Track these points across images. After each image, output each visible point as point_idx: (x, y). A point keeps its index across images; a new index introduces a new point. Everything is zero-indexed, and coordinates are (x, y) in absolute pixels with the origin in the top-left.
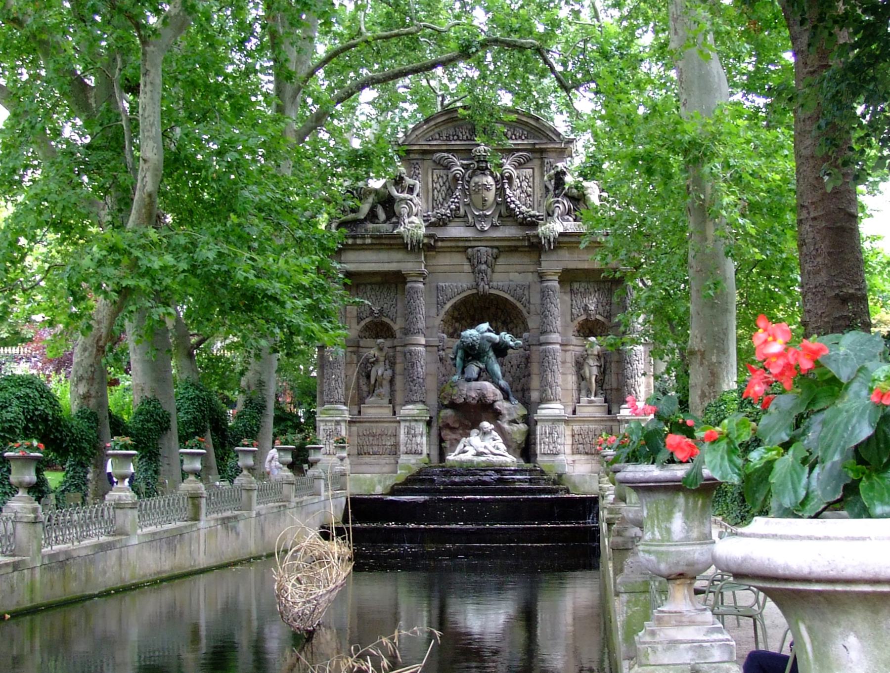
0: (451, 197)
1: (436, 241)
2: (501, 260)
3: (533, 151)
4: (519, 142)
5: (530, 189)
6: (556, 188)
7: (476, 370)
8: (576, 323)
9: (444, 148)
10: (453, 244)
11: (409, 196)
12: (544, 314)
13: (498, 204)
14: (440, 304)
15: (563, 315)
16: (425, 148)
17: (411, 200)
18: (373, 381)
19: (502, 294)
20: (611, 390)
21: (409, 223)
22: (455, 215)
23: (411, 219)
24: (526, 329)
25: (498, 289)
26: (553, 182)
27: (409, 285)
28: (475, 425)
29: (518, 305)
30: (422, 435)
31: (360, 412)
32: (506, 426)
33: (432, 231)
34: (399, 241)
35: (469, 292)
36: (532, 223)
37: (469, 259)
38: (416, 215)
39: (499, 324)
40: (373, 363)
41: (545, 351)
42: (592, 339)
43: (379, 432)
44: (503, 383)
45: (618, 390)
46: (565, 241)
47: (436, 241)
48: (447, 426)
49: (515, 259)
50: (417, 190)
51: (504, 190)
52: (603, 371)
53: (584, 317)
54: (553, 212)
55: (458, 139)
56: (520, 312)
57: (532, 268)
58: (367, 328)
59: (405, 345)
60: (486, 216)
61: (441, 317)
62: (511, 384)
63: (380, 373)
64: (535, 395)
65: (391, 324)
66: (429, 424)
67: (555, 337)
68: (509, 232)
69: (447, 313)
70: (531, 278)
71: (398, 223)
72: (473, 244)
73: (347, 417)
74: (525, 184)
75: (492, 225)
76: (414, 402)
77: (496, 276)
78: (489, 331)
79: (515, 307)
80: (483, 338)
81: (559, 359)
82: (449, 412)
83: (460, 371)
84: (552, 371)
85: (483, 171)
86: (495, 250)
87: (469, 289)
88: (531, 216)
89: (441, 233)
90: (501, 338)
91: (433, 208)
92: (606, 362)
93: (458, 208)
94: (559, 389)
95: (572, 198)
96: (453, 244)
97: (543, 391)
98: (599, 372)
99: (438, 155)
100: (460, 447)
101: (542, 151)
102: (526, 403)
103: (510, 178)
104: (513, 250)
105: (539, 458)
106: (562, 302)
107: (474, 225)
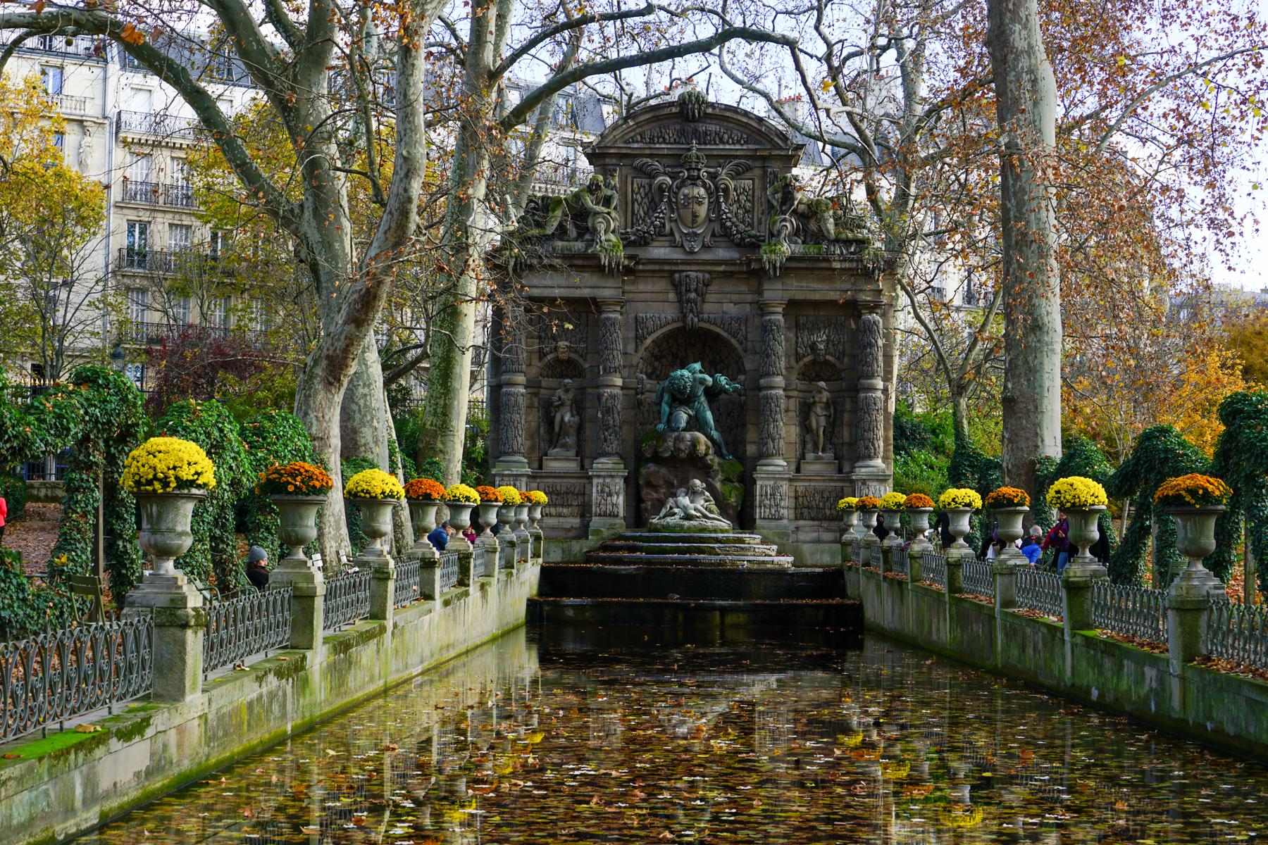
0: (655, 211)
1: (637, 263)
2: (712, 288)
3: (753, 157)
4: (738, 147)
5: (749, 204)
6: (783, 203)
7: (685, 416)
9: (647, 152)
10: (657, 267)
11: (606, 210)
12: (766, 353)
13: (711, 221)
14: (639, 339)
15: (787, 356)
16: (624, 151)
17: (609, 213)
18: (557, 429)
19: (712, 328)
20: (843, 444)
22: (660, 232)
24: (741, 370)
25: (709, 321)
26: (779, 196)
27: (604, 315)
28: (685, 483)
29: (733, 341)
30: (618, 495)
31: (540, 467)
32: (718, 485)
33: (631, 251)
34: (594, 262)
35: (675, 325)
36: (755, 246)
37: (676, 286)
38: (613, 232)
39: (706, 364)
40: (558, 406)
41: (767, 397)
42: (822, 384)
43: (564, 489)
44: (715, 434)
45: (852, 444)
46: (793, 267)
47: (637, 263)
48: (649, 484)
49: (729, 286)
50: (615, 203)
51: (719, 204)
52: (833, 424)
54: (779, 233)
55: (664, 142)
56: (735, 349)
57: (749, 298)
58: (550, 366)
59: (598, 387)
60: (695, 234)
61: (640, 355)
62: (722, 433)
63: (567, 418)
64: (751, 449)
65: (581, 360)
66: (626, 479)
67: (779, 380)
68: (722, 253)
69: (646, 349)
70: (748, 307)
71: (593, 240)
72: (681, 268)
73: (528, 470)
74: (743, 198)
75: (703, 246)
76: (605, 455)
77: (707, 307)
78: (701, 372)
79: (726, 343)
80: (695, 379)
81: (783, 406)
82: (652, 467)
83: (664, 420)
84: (775, 421)
85: (694, 180)
86: (707, 276)
87: (674, 321)
88: (749, 236)
89: (643, 254)
90: (715, 381)
91: (633, 224)
92: (835, 411)
93: (664, 224)
94: (782, 442)
96: (657, 267)
97: (762, 442)
98: (828, 422)
99: (637, 162)
100: (664, 511)
101: (763, 158)
102: (740, 457)
103: (726, 190)
104: (727, 275)
105: (758, 522)
106: (787, 340)
107: (682, 246)
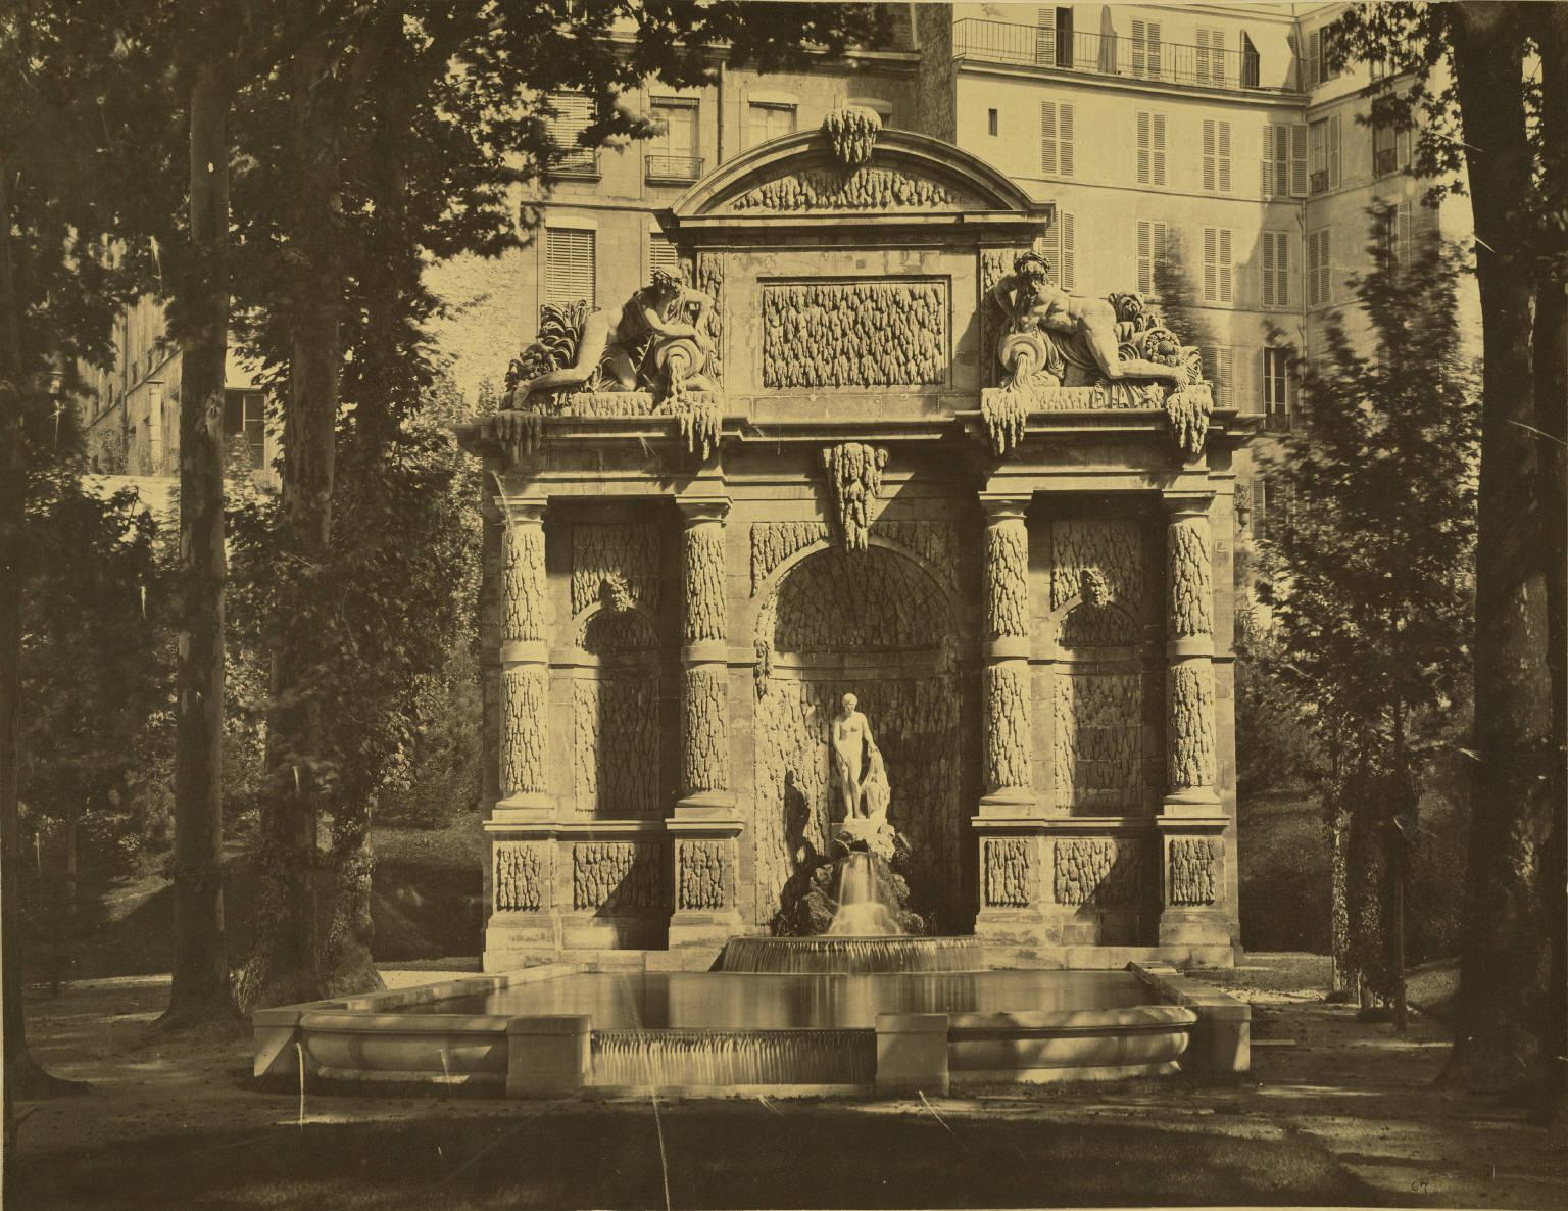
8: (1062, 615)
17: (692, 338)
21: (689, 389)
23: (692, 382)
35: (822, 545)
53: (1078, 600)
86: (883, 452)
95: (1057, 333)
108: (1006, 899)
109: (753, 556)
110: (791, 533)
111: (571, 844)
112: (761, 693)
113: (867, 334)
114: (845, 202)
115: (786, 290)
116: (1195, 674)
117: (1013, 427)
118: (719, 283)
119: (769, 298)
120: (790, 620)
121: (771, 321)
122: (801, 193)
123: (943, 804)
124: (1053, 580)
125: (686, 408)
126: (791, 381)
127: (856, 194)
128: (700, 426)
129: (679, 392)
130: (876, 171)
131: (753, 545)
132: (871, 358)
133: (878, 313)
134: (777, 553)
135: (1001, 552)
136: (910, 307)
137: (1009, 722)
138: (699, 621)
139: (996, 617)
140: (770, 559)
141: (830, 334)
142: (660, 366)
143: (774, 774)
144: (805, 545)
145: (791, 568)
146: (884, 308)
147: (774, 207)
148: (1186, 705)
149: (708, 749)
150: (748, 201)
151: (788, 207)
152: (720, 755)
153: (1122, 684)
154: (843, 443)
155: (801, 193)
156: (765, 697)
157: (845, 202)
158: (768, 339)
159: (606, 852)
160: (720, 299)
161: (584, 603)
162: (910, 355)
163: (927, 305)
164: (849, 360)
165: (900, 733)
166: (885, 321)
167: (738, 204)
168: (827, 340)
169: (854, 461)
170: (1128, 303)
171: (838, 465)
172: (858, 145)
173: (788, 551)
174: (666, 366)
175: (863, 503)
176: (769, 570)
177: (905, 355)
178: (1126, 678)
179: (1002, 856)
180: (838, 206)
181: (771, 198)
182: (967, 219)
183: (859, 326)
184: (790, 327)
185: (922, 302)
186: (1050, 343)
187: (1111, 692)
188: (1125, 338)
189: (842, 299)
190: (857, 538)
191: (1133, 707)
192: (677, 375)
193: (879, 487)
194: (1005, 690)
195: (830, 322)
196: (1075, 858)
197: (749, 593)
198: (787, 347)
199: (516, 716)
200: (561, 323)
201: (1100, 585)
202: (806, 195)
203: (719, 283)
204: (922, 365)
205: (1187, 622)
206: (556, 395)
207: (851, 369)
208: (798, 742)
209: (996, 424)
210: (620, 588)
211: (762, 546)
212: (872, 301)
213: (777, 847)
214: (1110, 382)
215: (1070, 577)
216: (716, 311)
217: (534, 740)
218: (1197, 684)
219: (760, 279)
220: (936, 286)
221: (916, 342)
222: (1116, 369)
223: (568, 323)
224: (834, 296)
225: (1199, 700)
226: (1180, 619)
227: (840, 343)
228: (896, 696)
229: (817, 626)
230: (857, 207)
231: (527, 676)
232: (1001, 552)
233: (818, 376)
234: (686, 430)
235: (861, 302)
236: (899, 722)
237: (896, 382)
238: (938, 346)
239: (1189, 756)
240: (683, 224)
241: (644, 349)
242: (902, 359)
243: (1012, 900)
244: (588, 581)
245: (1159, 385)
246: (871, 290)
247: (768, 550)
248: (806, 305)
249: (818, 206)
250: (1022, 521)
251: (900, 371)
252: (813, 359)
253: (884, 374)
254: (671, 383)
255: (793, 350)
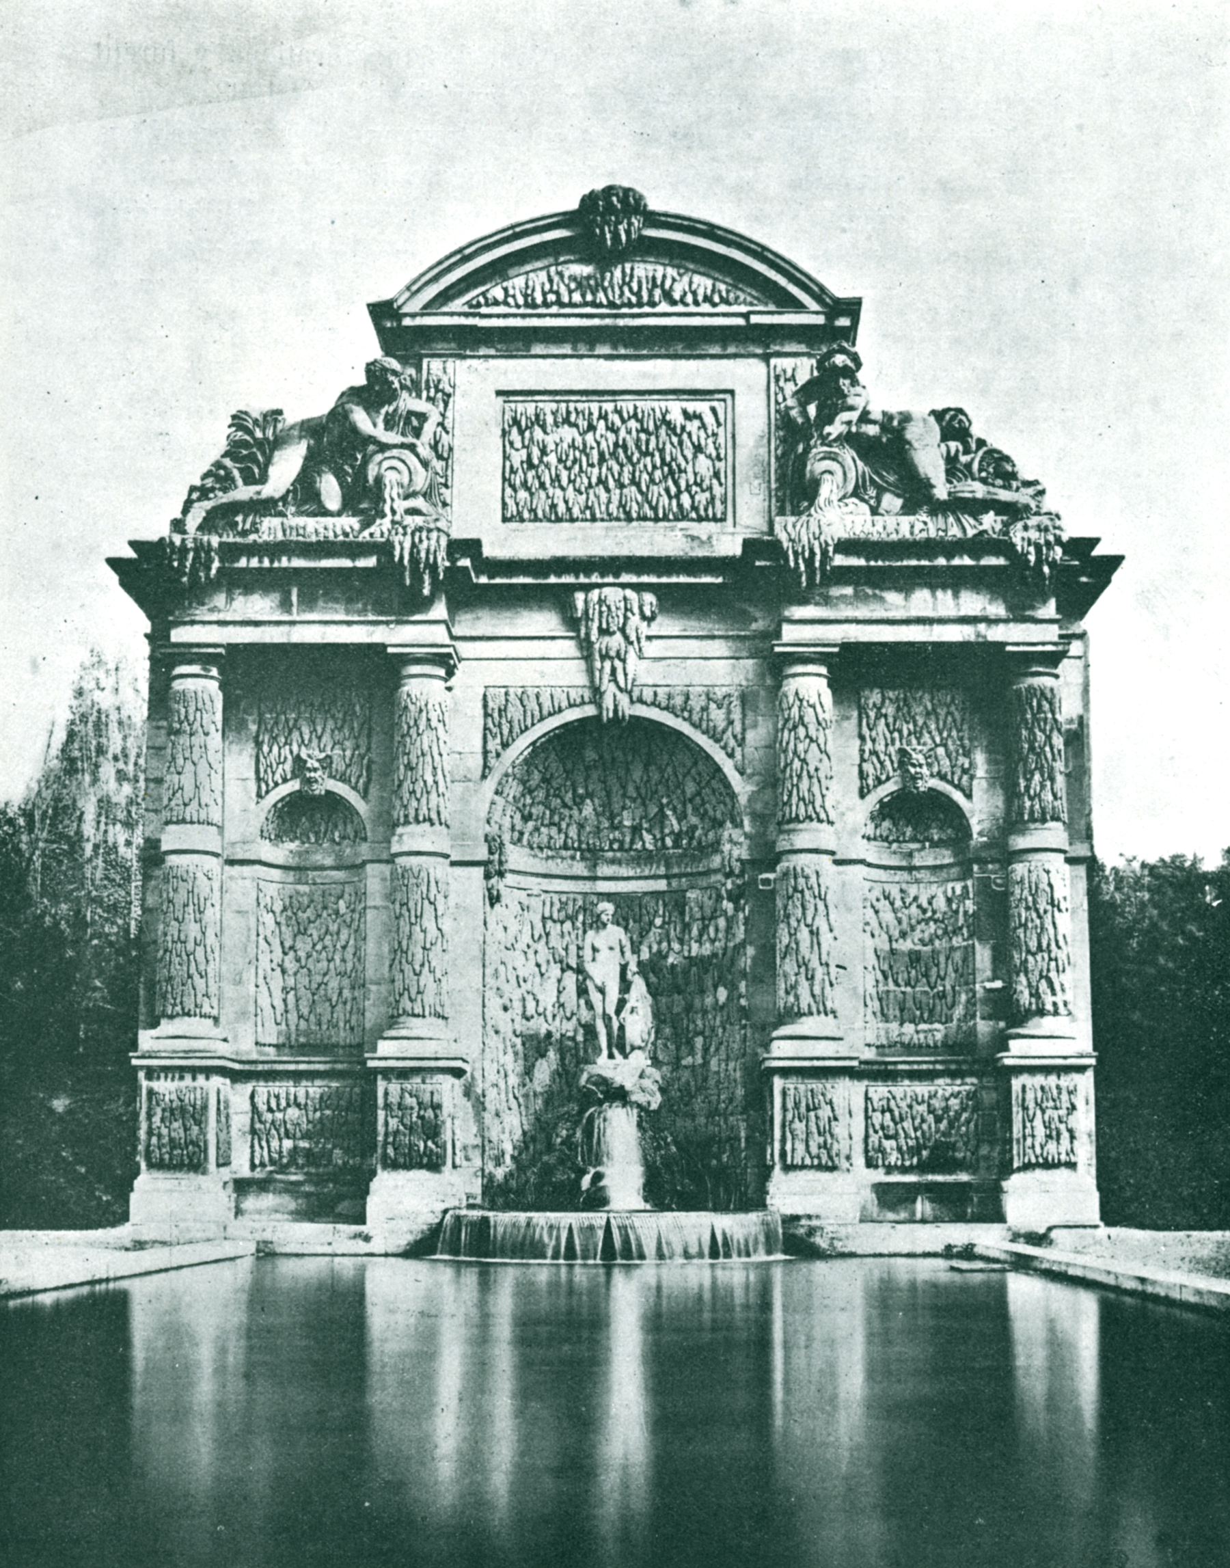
8: (872, 800)
23: (411, 503)
86: (649, 598)
108: (808, 1161)
109: (486, 728)
110: (533, 698)
111: (249, 1087)
112: (494, 899)
113: (629, 459)
114: (605, 302)
115: (531, 409)
116: (1048, 872)
117: (818, 557)
118: (449, 396)
119: (508, 416)
120: (530, 815)
121: (511, 444)
122: (551, 291)
123: (721, 1043)
124: (863, 760)
125: (401, 530)
126: (536, 515)
127: (617, 292)
128: (419, 552)
129: (394, 512)
130: (642, 265)
131: (486, 715)
132: (634, 489)
133: (643, 436)
134: (516, 724)
135: (801, 718)
136: (683, 428)
137: (811, 932)
138: (414, 804)
139: (794, 800)
140: (506, 731)
141: (584, 459)
142: (371, 479)
143: (509, 1004)
144: (550, 714)
145: (533, 743)
146: (651, 428)
147: (518, 306)
148: (1037, 910)
149: (422, 965)
150: (486, 299)
151: (535, 306)
152: (438, 975)
153: (945, 892)
154: (600, 586)
155: (551, 291)
156: (497, 906)
157: (605, 302)
158: (508, 464)
159: (292, 1097)
160: (449, 414)
161: (271, 784)
162: (683, 485)
163: (703, 426)
164: (608, 490)
165: (666, 957)
166: (652, 445)
167: (474, 302)
168: (581, 467)
169: (613, 609)
170: (953, 418)
171: (594, 613)
172: (622, 228)
173: (529, 722)
174: (379, 480)
175: (624, 661)
176: (505, 745)
177: (676, 483)
178: (950, 885)
179: (803, 1104)
180: (594, 304)
181: (514, 296)
182: (754, 319)
183: (620, 451)
184: (536, 452)
185: (697, 423)
186: (860, 464)
187: (930, 903)
188: (951, 460)
189: (600, 417)
190: (616, 706)
191: (961, 921)
192: (391, 491)
193: (643, 642)
194: (807, 893)
195: (585, 444)
196: (891, 1111)
197: (479, 773)
198: (531, 474)
199: (176, 919)
200: (250, 432)
201: (920, 766)
202: (557, 293)
203: (449, 396)
204: (697, 498)
205: (1037, 807)
206: (239, 518)
207: (609, 502)
208: (538, 965)
209: (796, 553)
210: (317, 765)
211: (496, 715)
212: (637, 420)
213: (511, 1096)
214: (938, 508)
215: (882, 757)
216: (444, 429)
217: (200, 952)
218: (1050, 885)
219: (499, 393)
220: (715, 404)
221: (690, 469)
222: (941, 492)
223: (259, 434)
224: (591, 414)
225: (1053, 906)
226: (1028, 804)
227: (596, 471)
228: (661, 912)
229: (564, 825)
230: (619, 307)
231: (191, 869)
232: (801, 718)
233: (569, 509)
234: (402, 557)
235: (623, 421)
236: (665, 945)
237: (665, 518)
238: (716, 475)
239: (1041, 977)
240: (407, 322)
241: (352, 467)
242: (673, 490)
243: (816, 1162)
244: (280, 754)
245: (997, 514)
246: (636, 408)
247: (504, 721)
248: (556, 424)
249: (572, 305)
250: (824, 682)
251: (670, 504)
252: (563, 489)
253: (651, 507)
254: (385, 501)
255: (539, 477)
